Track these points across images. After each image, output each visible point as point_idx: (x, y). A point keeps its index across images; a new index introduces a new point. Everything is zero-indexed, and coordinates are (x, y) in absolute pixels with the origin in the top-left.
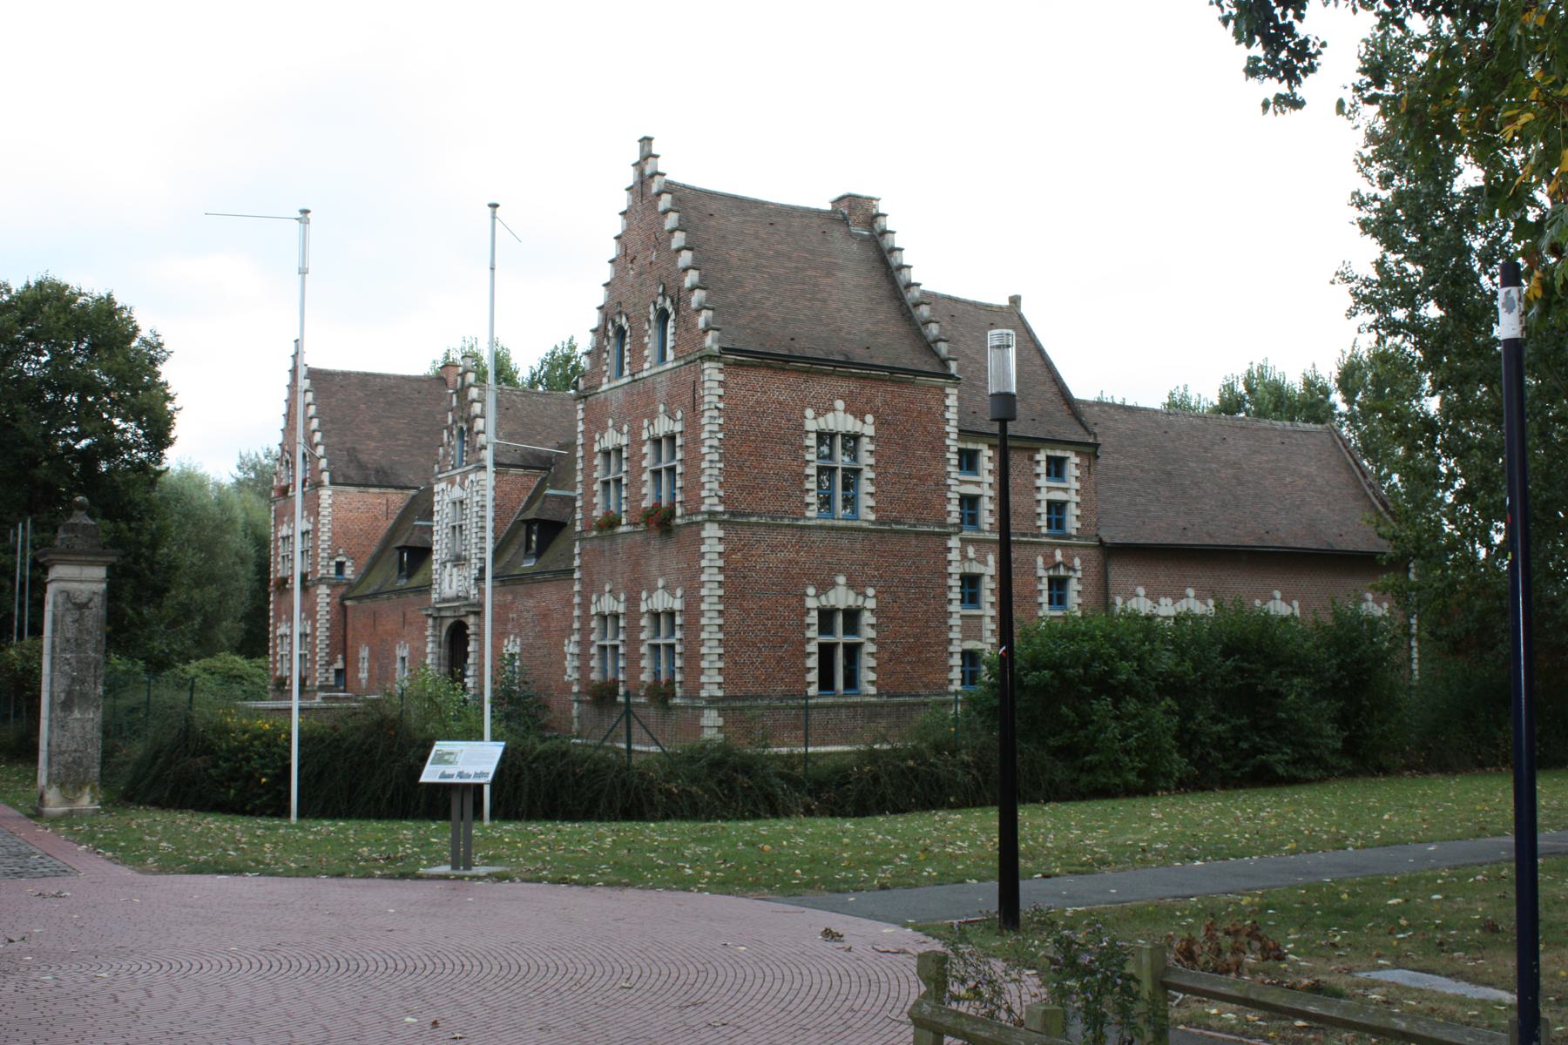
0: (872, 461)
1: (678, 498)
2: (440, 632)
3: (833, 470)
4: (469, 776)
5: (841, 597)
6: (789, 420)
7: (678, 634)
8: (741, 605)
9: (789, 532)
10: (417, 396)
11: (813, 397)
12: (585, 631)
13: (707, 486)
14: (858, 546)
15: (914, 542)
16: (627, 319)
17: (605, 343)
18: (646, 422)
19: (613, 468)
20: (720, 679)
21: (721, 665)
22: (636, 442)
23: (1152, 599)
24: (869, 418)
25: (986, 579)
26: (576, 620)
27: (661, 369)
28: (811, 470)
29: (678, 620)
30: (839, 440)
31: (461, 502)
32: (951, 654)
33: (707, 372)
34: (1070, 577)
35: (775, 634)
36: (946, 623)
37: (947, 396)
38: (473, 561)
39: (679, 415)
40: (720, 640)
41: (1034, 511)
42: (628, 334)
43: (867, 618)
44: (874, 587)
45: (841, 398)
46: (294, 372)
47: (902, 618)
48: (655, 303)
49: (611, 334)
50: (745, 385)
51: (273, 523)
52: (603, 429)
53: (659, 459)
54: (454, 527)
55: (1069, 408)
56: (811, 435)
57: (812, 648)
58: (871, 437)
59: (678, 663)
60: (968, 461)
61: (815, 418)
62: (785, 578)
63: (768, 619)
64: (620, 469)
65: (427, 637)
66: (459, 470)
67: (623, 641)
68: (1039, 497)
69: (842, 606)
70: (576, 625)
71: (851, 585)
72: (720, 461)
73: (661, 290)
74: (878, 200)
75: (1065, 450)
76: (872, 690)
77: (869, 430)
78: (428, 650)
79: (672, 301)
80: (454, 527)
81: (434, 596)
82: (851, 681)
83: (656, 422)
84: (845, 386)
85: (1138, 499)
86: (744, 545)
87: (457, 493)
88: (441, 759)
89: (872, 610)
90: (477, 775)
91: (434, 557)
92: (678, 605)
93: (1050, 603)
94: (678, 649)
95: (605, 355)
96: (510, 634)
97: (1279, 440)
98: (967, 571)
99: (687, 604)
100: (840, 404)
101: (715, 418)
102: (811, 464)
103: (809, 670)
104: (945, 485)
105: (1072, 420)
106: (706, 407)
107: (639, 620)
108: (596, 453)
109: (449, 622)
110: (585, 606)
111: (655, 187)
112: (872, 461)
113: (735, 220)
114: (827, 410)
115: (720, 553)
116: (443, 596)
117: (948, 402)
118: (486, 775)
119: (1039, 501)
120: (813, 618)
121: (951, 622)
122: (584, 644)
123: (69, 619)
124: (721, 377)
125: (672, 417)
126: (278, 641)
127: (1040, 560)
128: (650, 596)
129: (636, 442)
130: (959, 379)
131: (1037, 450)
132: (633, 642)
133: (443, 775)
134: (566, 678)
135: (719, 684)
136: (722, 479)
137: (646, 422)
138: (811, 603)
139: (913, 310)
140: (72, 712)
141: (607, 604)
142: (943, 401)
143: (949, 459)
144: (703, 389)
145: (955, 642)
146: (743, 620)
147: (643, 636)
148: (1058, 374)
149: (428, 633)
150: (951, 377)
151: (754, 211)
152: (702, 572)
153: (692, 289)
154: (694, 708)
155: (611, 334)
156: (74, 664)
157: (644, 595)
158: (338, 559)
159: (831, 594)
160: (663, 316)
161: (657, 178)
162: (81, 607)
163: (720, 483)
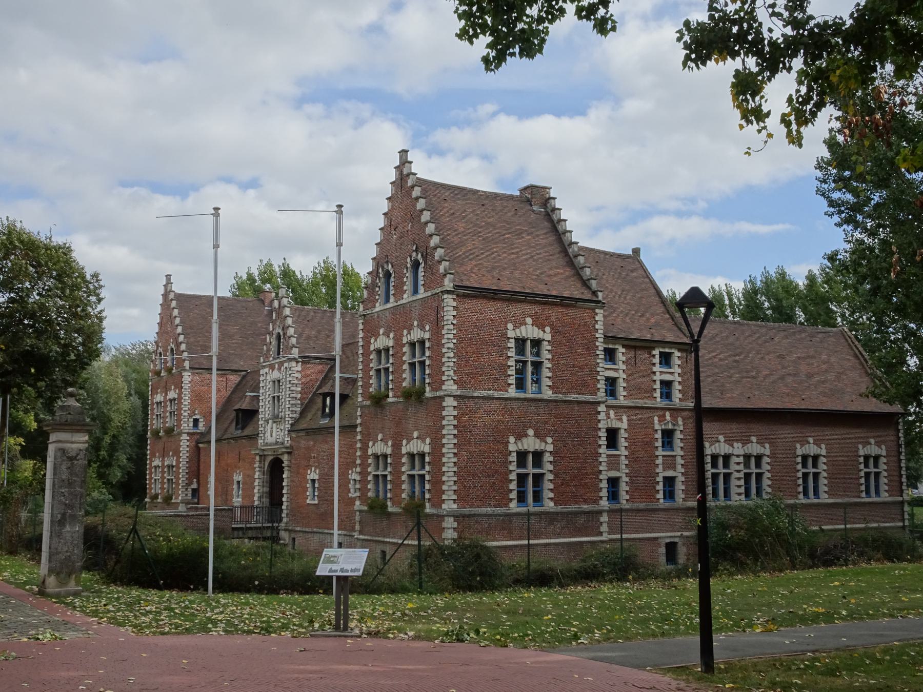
0: (549, 356)
1: (427, 381)
2: (264, 464)
3: (525, 362)
4: (347, 571)
5: (531, 443)
6: (497, 331)
7: (427, 468)
8: (468, 449)
9: (498, 402)
10: (245, 311)
12: (364, 465)
13: (446, 373)
14: (542, 411)
15: (576, 408)
16: (392, 266)
17: (378, 281)
18: (405, 332)
19: (383, 361)
20: (455, 497)
21: (455, 488)
22: (398, 344)
23: (728, 444)
24: (548, 329)
25: (622, 431)
26: (358, 458)
27: (414, 298)
29: (427, 459)
30: (529, 343)
31: (279, 381)
33: (445, 301)
35: (489, 468)
36: (597, 460)
37: (597, 314)
38: (287, 419)
39: (427, 328)
40: (455, 472)
42: (393, 276)
43: (548, 457)
45: (530, 316)
46: (165, 295)
47: (569, 457)
48: (411, 257)
49: (381, 275)
51: (150, 393)
52: (377, 336)
53: (414, 356)
54: (274, 397)
55: (673, 320)
56: (511, 340)
57: (513, 477)
58: (549, 341)
59: (427, 486)
60: (610, 355)
64: (388, 362)
65: (255, 468)
66: (278, 361)
67: (390, 472)
68: (655, 378)
69: (532, 450)
70: (358, 462)
71: (537, 435)
72: (454, 357)
73: (414, 248)
75: (671, 348)
76: (552, 504)
77: (548, 337)
78: (256, 476)
79: (422, 255)
80: (274, 397)
81: (260, 441)
82: (537, 497)
83: (412, 332)
85: (719, 379)
86: (470, 411)
87: (276, 375)
88: (329, 560)
89: (551, 452)
90: (352, 570)
91: (260, 416)
92: (427, 449)
93: (663, 446)
94: (427, 477)
95: (377, 289)
96: (312, 467)
97: (808, 339)
98: (610, 426)
99: (433, 449)
100: (529, 320)
101: (451, 330)
103: (511, 491)
104: (596, 371)
105: (676, 328)
106: (445, 323)
107: (401, 459)
108: (372, 351)
109: (270, 458)
110: (365, 448)
111: (410, 183)
113: (459, 202)
114: (521, 324)
115: (454, 416)
116: (266, 441)
117: (597, 318)
118: (359, 570)
119: (655, 381)
120: (513, 457)
121: (601, 459)
122: (364, 473)
123: (64, 467)
124: (455, 304)
125: (422, 328)
126: (153, 470)
127: (656, 419)
128: (408, 443)
129: (398, 344)
130: (604, 303)
131: (654, 348)
132: (397, 473)
133: (331, 571)
134: (350, 495)
135: (454, 500)
136: (456, 369)
137: (405, 332)
138: (512, 447)
139: (573, 260)
140: (65, 526)
141: (380, 447)
142: (594, 318)
144: (444, 312)
145: (603, 473)
146: (469, 459)
147: (403, 469)
149: (255, 466)
150: (599, 302)
151: (472, 197)
152: (443, 428)
153: (435, 248)
154: (438, 516)
155: (381, 275)
156: (67, 495)
157: (404, 442)
158: (194, 417)
159: (525, 440)
160: (416, 264)
161: (411, 176)
162: (71, 459)
163: (455, 371)
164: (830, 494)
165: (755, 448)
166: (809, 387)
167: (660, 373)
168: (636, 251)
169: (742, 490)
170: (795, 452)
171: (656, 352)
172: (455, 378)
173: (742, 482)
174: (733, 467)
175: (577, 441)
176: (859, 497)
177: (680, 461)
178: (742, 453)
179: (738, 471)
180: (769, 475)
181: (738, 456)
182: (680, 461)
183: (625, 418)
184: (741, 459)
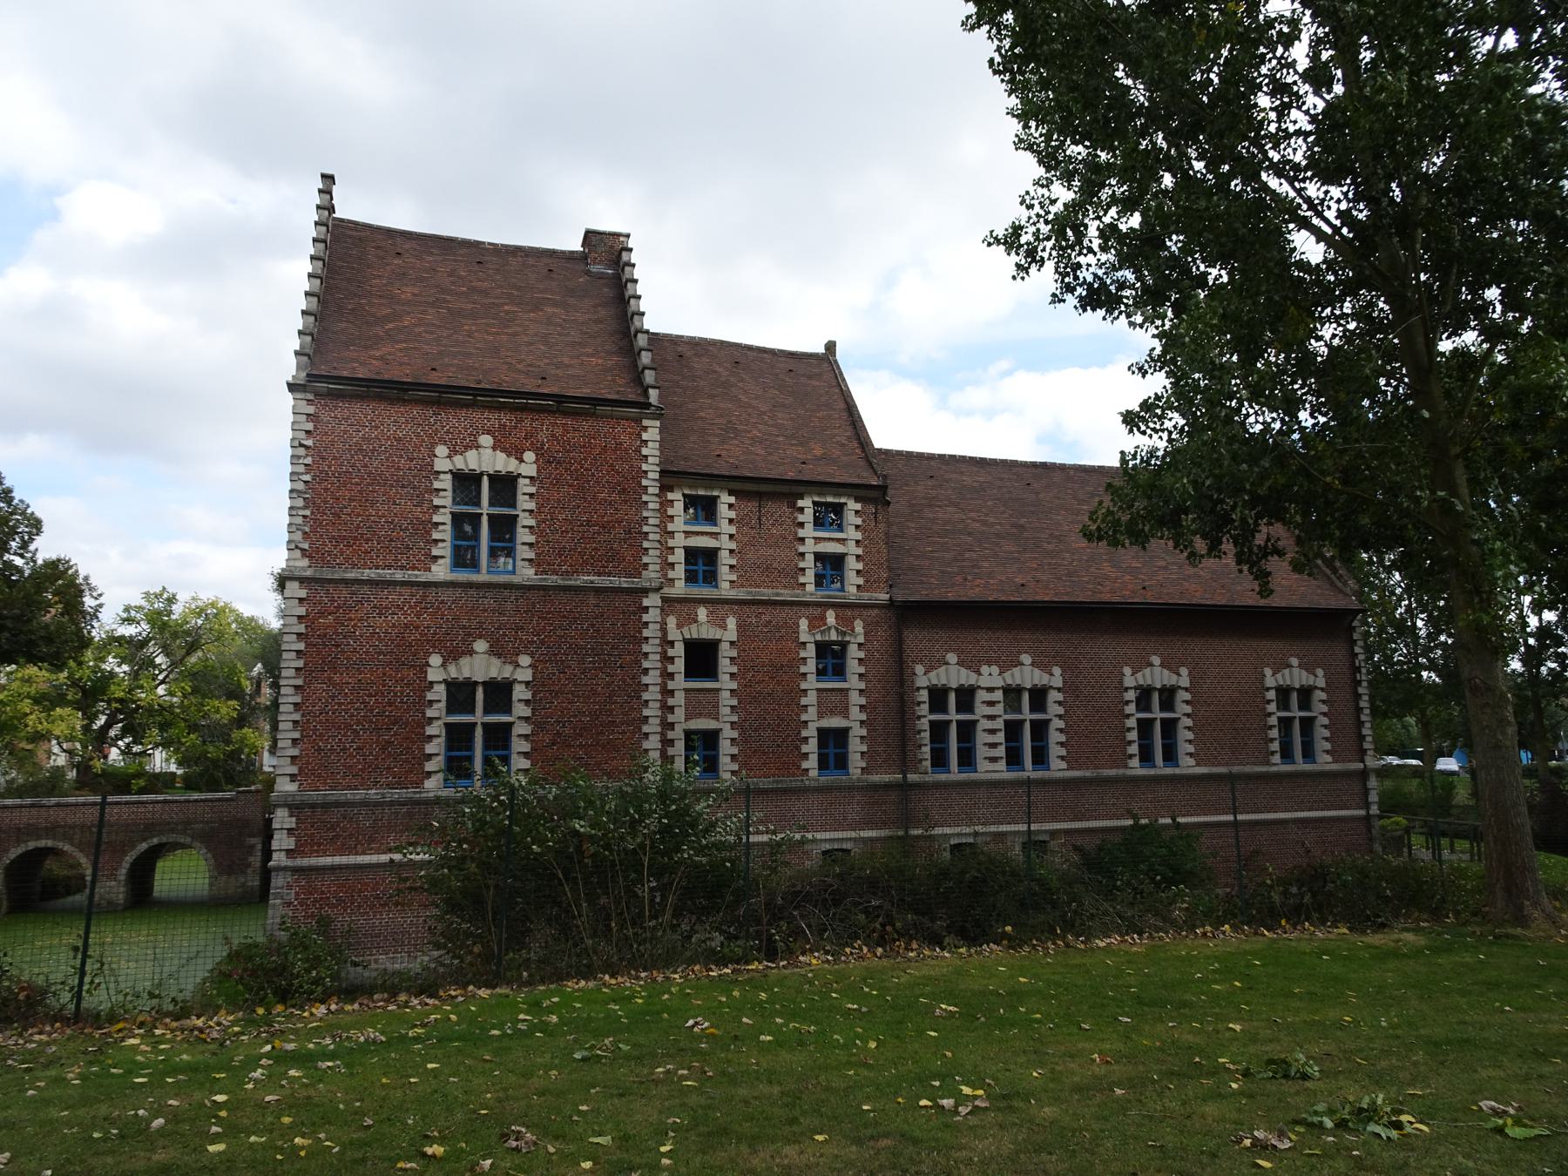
5: (480, 666)
8: (330, 679)
9: (406, 591)
11: (448, 432)
14: (509, 606)
15: (592, 601)
20: (294, 770)
24: (529, 456)
25: (724, 646)
28: (444, 517)
30: (485, 481)
32: (646, 735)
34: (849, 642)
37: (645, 429)
41: (796, 565)
44: (532, 655)
50: (346, 419)
55: (863, 451)
56: (442, 476)
58: (531, 478)
61: (449, 457)
62: (398, 645)
63: (370, 695)
68: (801, 549)
71: (496, 651)
72: (305, 508)
74: (628, 236)
75: (840, 495)
84: (493, 419)
86: (339, 607)
89: (527, 683)
102: (442, 510)
104: (640, 532)
112: (532, 505)
114: (467, 448)
115: (300, 617)
119: (802, 555)
120: (439, 692)
124: (311, 409)
127: (804, 624)
138: (434, 675)
142: (639, 435)
143: (646, 503)
148: (860, 417)
164: (1071, 761)
165: (1027, 675)
166: (1165, 568)
167: (813, 540)
168: (831, 347)
169: (1001, 751)
170: (1121, 682)
171: (806, 503)
172: (306, 546)
173: (1000, 737)
174: (981, 710)
175: (593, 662)
176: (1268, 763)
177: (856, 699)
178: (1000, 683)
179: (992, 718)
180: (1061, 724)
181: (991, 690)
182: (856, 699)
183: (732, 623)
184: (998, 695)
